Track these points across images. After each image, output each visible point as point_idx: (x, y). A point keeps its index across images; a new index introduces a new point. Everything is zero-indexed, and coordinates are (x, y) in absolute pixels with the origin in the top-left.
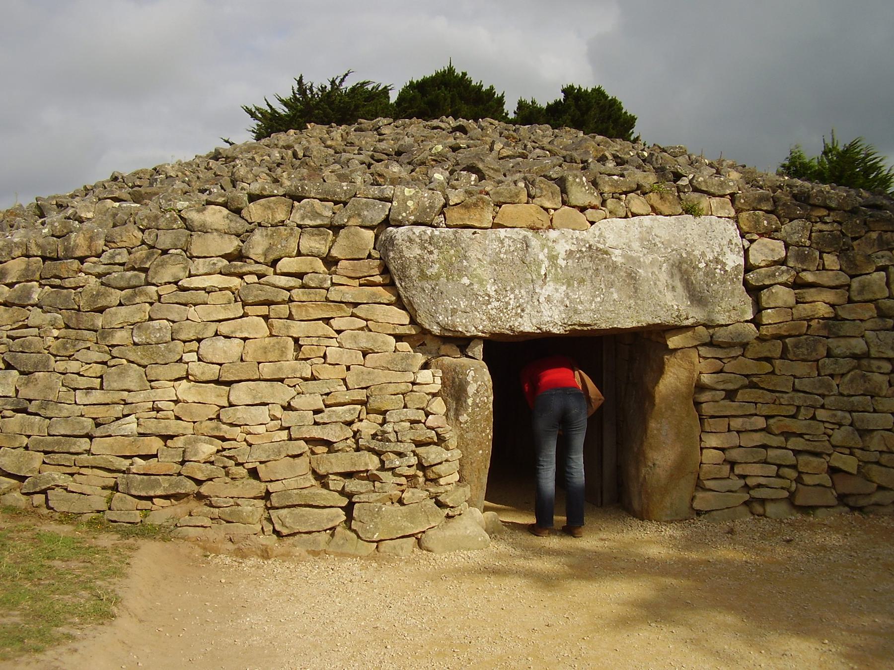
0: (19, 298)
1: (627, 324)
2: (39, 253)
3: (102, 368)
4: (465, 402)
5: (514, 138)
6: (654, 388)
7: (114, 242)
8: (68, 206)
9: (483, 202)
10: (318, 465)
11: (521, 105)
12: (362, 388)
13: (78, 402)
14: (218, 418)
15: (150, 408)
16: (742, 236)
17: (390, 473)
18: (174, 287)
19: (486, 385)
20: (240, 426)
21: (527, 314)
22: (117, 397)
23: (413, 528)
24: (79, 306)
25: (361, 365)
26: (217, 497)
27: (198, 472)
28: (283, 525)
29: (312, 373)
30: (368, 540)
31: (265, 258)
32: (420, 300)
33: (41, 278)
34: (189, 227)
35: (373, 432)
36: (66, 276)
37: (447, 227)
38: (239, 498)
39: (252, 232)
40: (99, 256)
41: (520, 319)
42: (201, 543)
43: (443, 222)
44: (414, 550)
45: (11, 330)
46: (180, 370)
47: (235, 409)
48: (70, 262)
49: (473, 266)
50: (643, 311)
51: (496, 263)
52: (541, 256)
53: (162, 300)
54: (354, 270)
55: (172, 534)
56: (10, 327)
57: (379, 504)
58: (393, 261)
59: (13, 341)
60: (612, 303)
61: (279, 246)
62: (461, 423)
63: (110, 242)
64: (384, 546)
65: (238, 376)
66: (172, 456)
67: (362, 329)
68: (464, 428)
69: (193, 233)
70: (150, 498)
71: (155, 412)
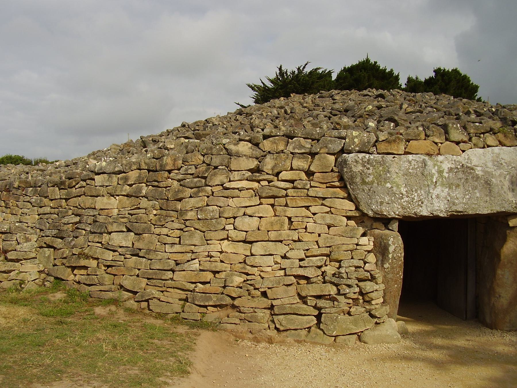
0: (135, 192)
1: (485, 211)
2: (146, 168)
3: (180, 232)
4: (388, 256)
5: (413, 101)
6: (500, 250)
7: (187, 162)
8: (159, 141)
9: (399, 139)
10: (301, 290)
11: (410, 80)
12: (327, 247)
13: (166, 251)
14: (245, 262)
15: (206, 256)
17: (343, 297)
18: (221, 188)
19: (400, 247)
20: (257, 267)
21: (425, 205)
22: (188, 248)
23: (356, 329)
24: (168, 197)
25: (327, 234)
26: (244, 307)
27: (233, 292)
28: (281, 325)
29: (299, 237)
30: (330, 335)
31: (272, 171)
32: (362, 196)
33: (147, 182)
34: (229, 153)
35: (333, 272)
36: (161, 181)
37: (378, 154)
38: (256, 308)
39: (265, 157)
40: (179, 170)
41: (420, 208)
42: (234, 333)
43: (376, 151)
44: (356, 342)
45: (130, 210)
46: (223, 234)
47: (254, 257)
48: (163, 173)
49: (393, 176)
50: (495, 204)
51: (407, 175)
52: (433, 171)
53: (214, 194)
54: (323, 179)
55: (218, 327)
56: (130, 208)
57: (336, 315)
58: (346, 174)
59: (132, 216)
60: (476, 199)
61: (281, 165)
62: (385, 268)
63: (185, 162)
64: (339, 339)
65: (256, 238)
66: (219, 283)
67: (327, 213)
68: (387, 271)
69: (232, 157)
70: (206, 307)
71: (209, 258)
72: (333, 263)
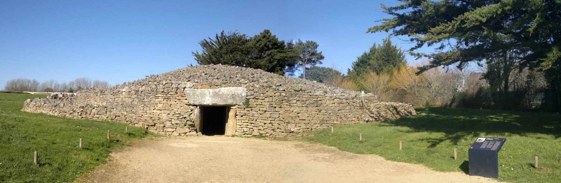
16: (247, 90)
46: (154, 108)
72: (181, 116)
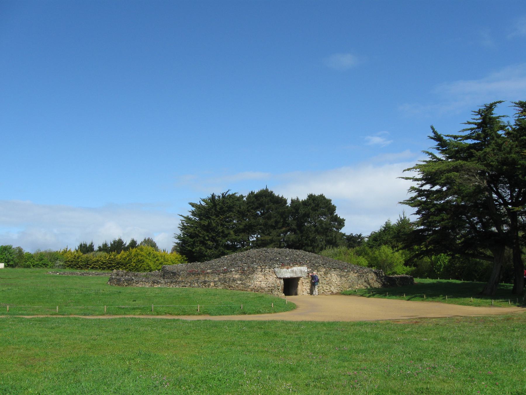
11: (293, 201)
